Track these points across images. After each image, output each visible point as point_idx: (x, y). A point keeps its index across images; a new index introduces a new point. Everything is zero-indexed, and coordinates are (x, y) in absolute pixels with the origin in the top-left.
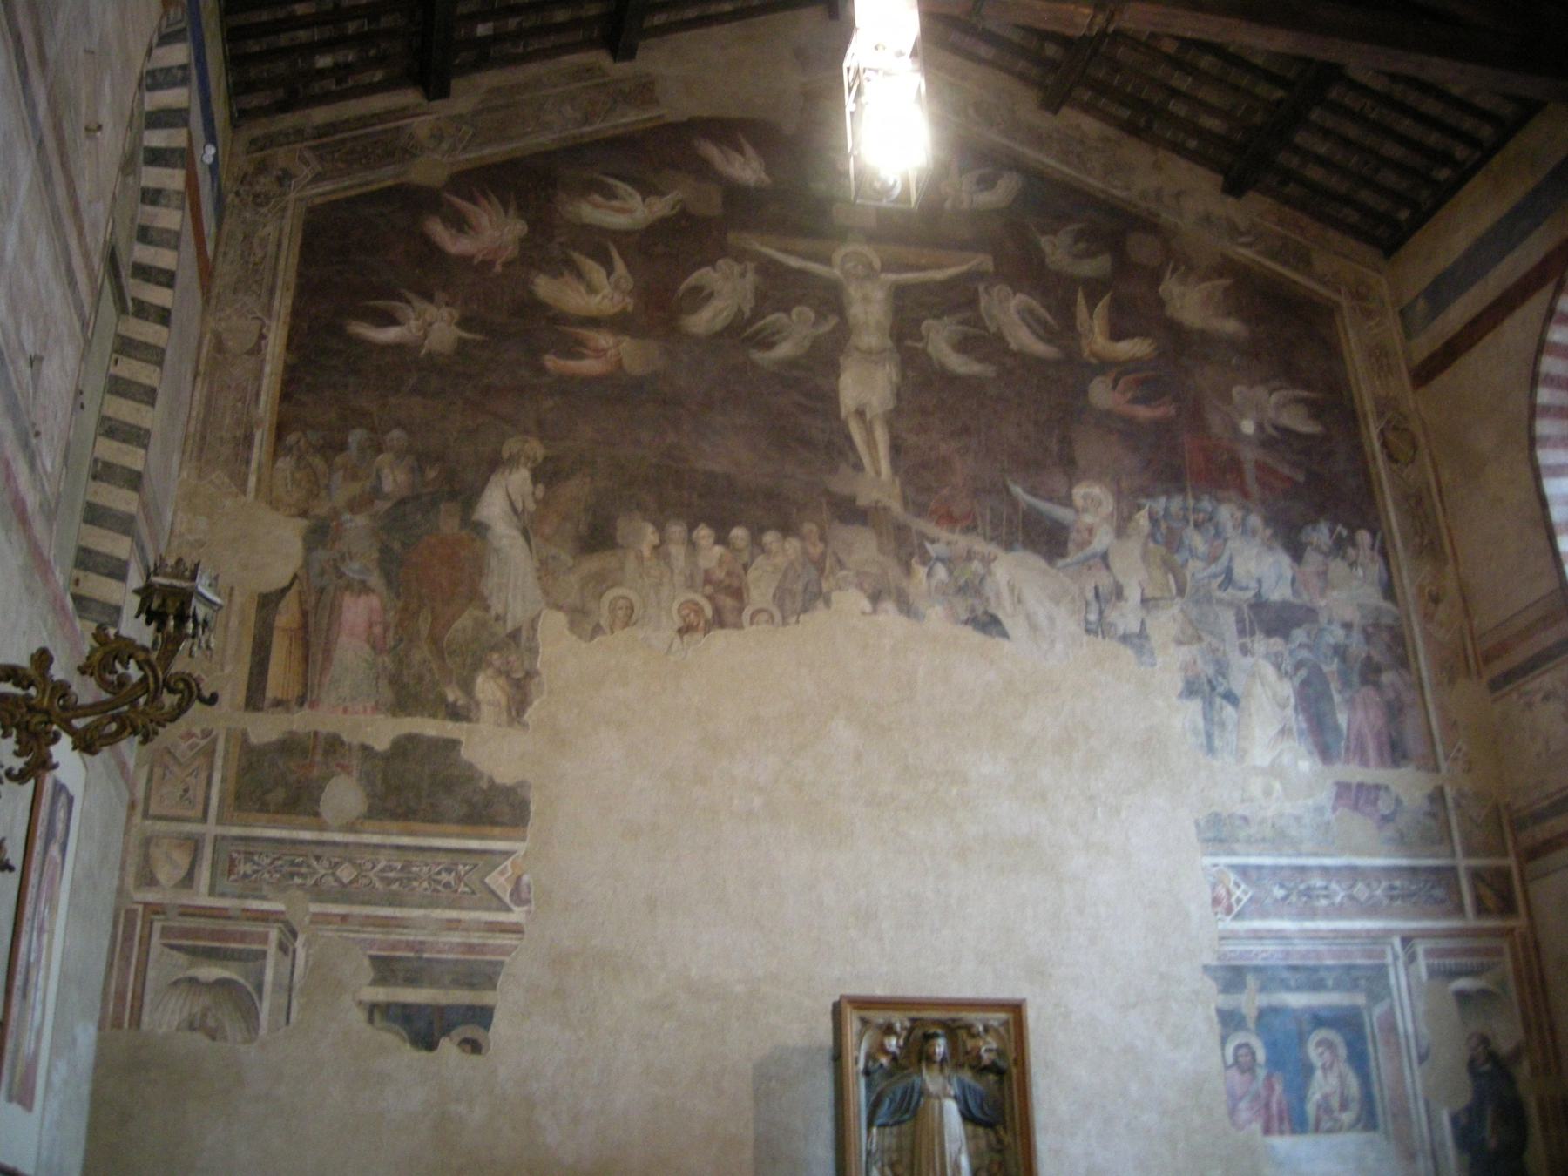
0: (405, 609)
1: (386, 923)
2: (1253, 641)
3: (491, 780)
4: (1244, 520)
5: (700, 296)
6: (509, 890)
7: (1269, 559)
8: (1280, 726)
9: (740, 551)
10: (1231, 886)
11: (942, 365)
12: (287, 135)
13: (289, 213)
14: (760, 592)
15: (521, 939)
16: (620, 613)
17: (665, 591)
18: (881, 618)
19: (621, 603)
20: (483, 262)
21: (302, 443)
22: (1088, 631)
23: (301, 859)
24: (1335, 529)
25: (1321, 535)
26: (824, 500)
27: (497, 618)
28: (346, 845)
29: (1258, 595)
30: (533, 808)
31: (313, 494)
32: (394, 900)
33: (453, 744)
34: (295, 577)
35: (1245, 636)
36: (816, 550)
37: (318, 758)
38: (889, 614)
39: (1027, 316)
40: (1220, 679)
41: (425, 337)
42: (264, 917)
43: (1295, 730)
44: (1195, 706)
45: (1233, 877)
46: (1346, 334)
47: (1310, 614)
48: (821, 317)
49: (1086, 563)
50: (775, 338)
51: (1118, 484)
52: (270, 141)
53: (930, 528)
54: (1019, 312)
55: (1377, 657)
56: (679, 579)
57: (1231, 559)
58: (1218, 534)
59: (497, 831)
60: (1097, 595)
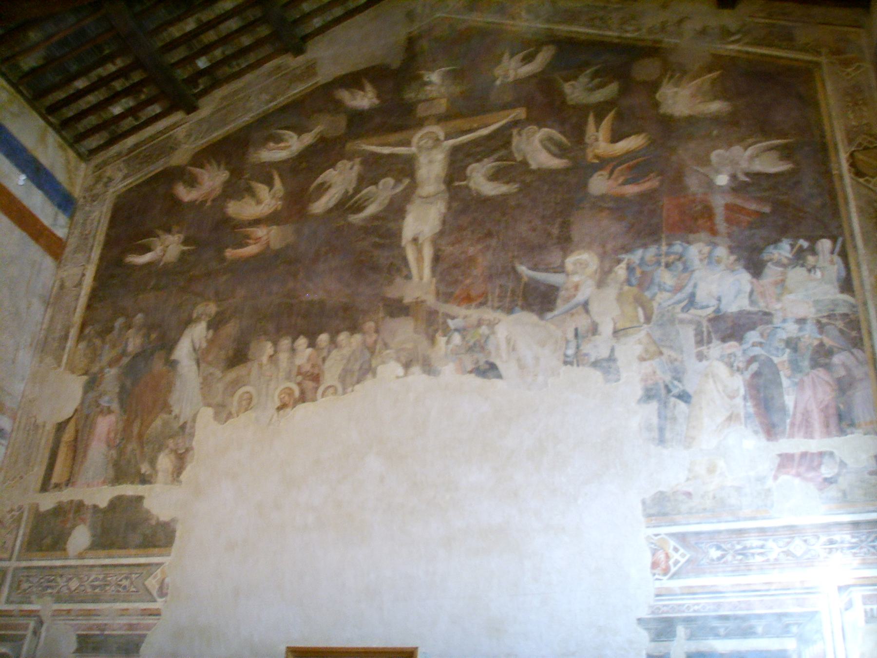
0: (127, 420)
1: (89, 614)
2: (709, 348)
3: (158, 519)
4: (710, 253)
5: (323, 188)
6: (157, 586)
7: (730, 279)
8: (728, 414)
9: (323, 349)
10: (671, 551)
11: (478, 193)
12: (113, 157)
13: (107, 202)
14: (331, 374)
15: (159, 619)
16: (244, 403)
17: (272, 385)
18: (410, 378)
19: (246, 396)
20: (201, 202)
21: (92, 332)
22: (566, 363)
23: (53, 578)
24: (797, 243)
25: (784, 250)
26: (381, 304)
27: (176, 417)
28: (76, 567)
29: (718, 310)
30: (178, 534)
31: (92, 361)
32: (96, 600)
33: (140, 499)
34: (76, 410)
35: (703, 345)
36: (371, 339)
37: (71, 516)
38: (417, 376)
39: (550, 145)
40: (676, 383)
41: (164, 255)
42: (29, 614)
43: (742, 414)
44: (654, 405)
45: (672, 543)
46: (824, 86)
47: (766, 316)
48: (398, 181)
49: (570, 312)
50: (366, 203)
51: (604, 247)
52: (105, 163)
53: (452, 308)
54: (541, 141)
55: (828, 342)
56: (282, 374)
57: (695, 286)
58: (685, 269)
59: (156, 550)
60: (576, 335)
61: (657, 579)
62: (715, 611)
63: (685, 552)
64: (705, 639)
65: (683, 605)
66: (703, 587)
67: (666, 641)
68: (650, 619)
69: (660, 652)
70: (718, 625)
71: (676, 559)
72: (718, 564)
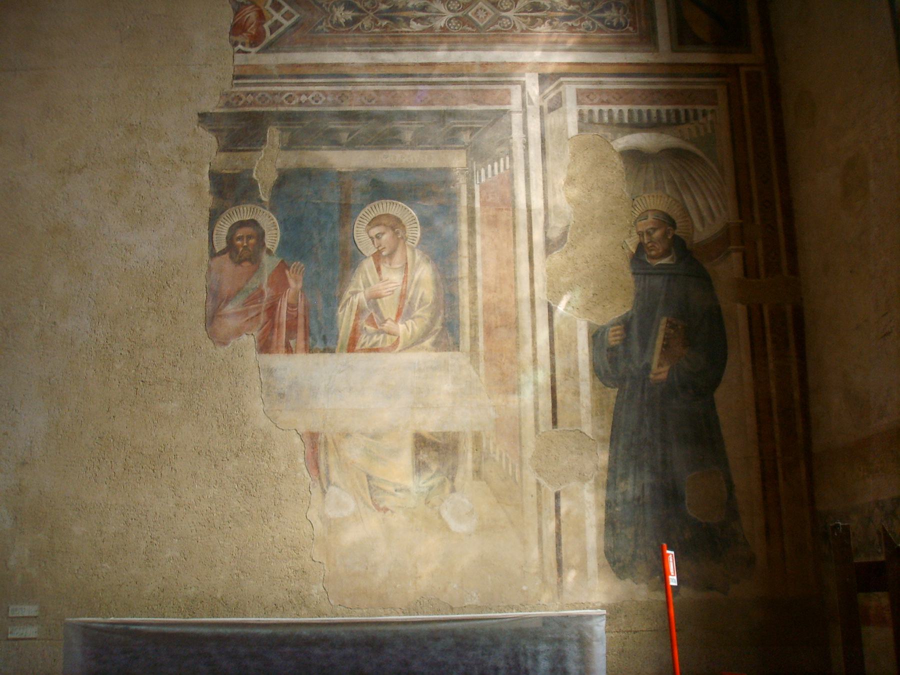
61: (239, 51)
62: (337, 105)
63: (292, 11)
64: (315, 149)
65: (283, 93)
66: (317, 65)
67: (247, 151)
68: (223, 114)
69: (235, 169)
70: (340, 127)
71: (276, 21)
72: (347, 32)
